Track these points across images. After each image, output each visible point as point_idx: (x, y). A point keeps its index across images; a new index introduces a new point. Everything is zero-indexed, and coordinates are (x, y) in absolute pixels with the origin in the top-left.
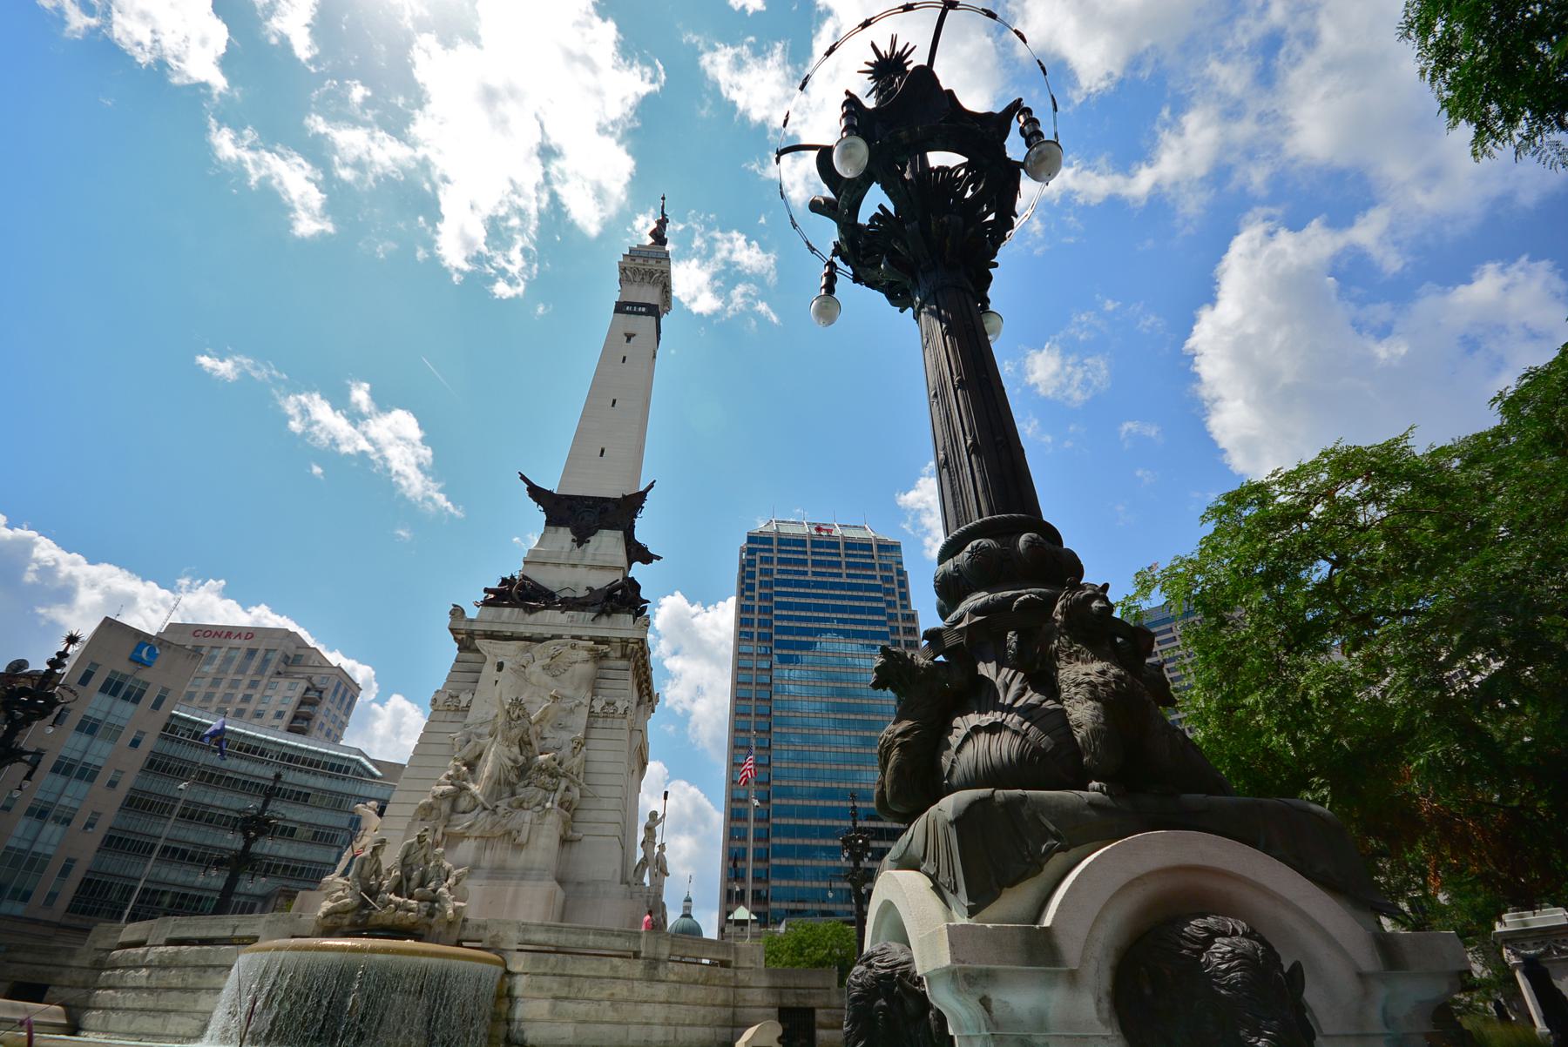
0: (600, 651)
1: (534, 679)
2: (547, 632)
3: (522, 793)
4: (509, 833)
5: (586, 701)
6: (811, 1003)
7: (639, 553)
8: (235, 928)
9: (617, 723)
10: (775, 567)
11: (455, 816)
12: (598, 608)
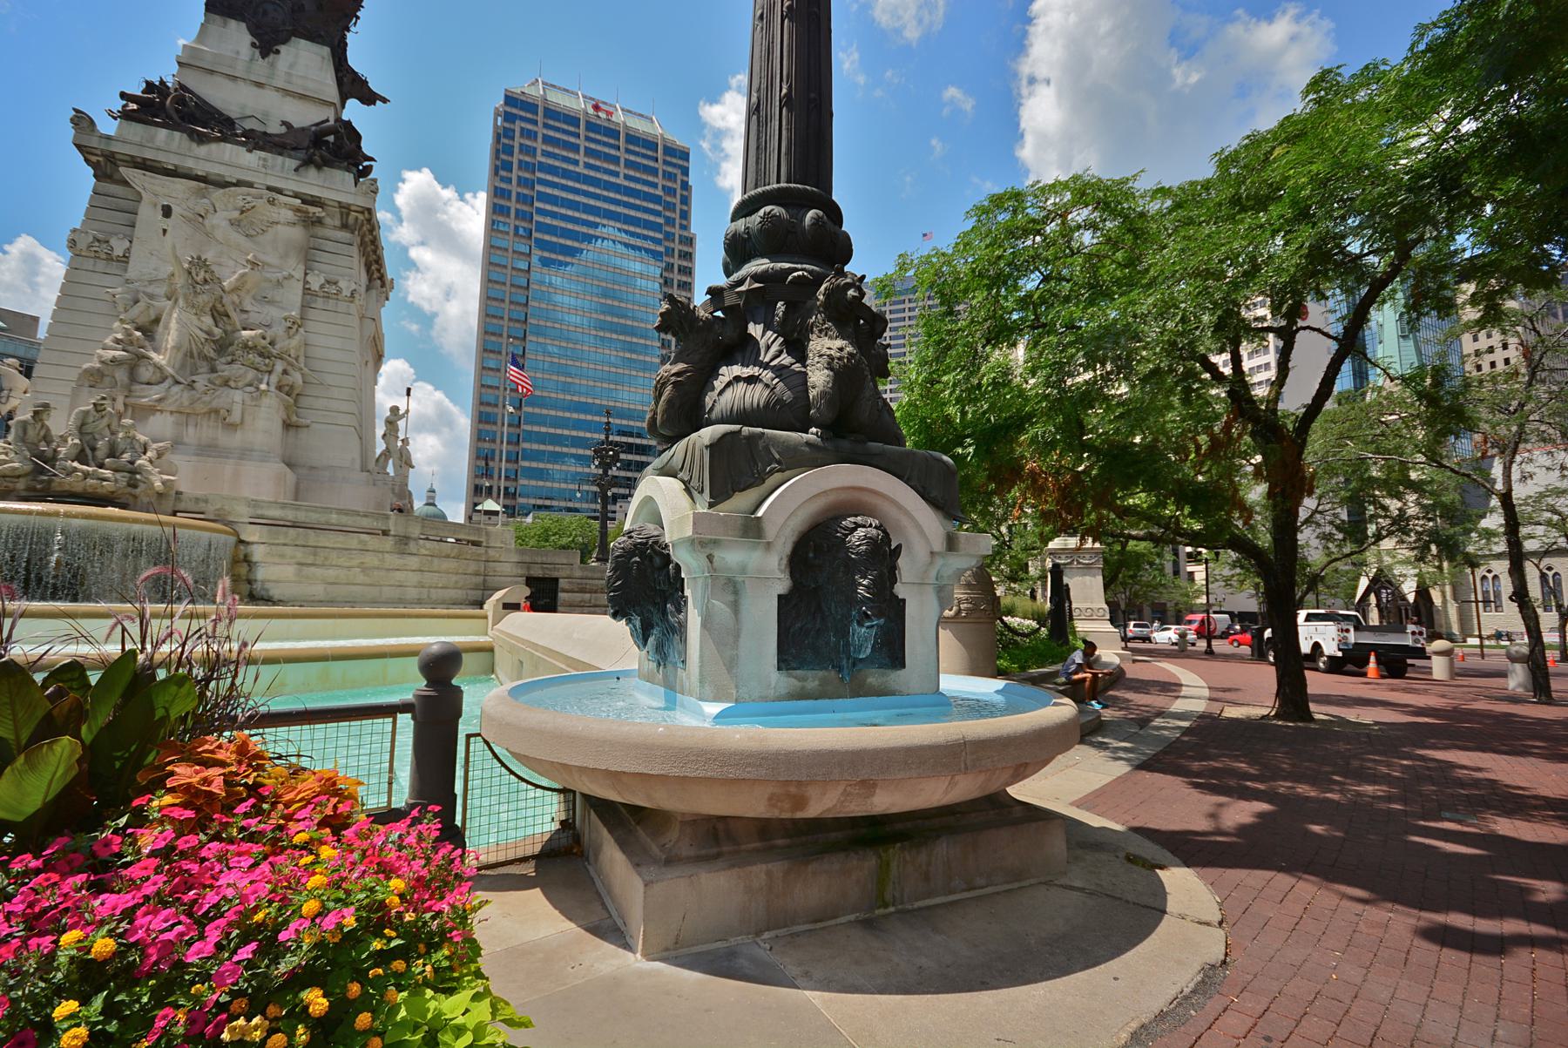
0: (310, 210)
1: (219, 234)
2: (231, 175)
3: (226, 371)
4: (217, 412)
5: (299, 274)
6: (555, 574)
7: (353, 86)
9: (342, 307)
10: (539, 146)
11: (137, 387)
12: (301, 154)
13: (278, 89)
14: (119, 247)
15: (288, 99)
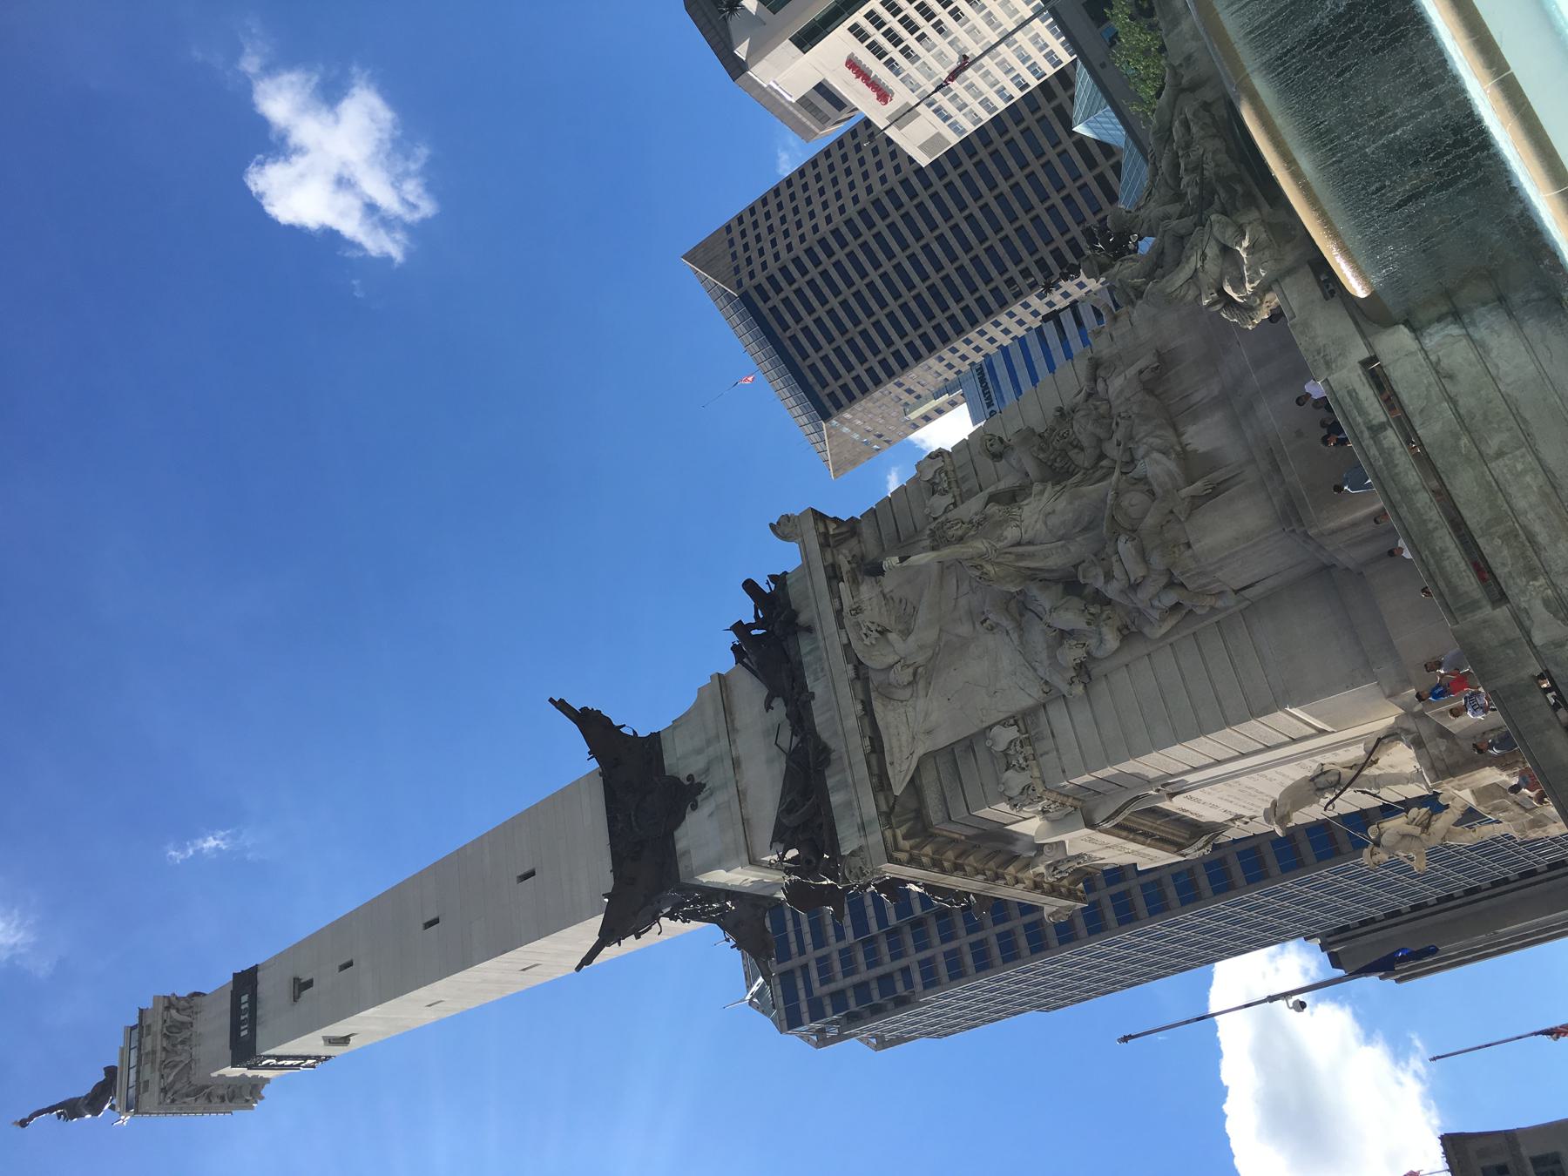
1: (930, 635)
8: (1376, 430)
13: (731, 742)
14: (1005, 736)
15: (738, 724)
